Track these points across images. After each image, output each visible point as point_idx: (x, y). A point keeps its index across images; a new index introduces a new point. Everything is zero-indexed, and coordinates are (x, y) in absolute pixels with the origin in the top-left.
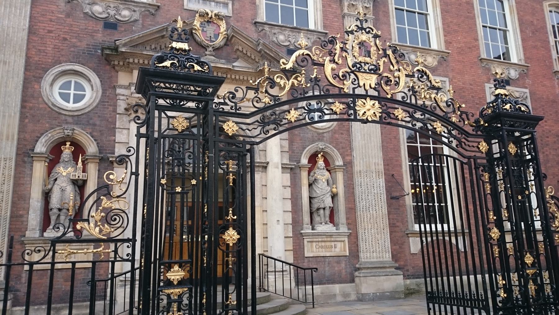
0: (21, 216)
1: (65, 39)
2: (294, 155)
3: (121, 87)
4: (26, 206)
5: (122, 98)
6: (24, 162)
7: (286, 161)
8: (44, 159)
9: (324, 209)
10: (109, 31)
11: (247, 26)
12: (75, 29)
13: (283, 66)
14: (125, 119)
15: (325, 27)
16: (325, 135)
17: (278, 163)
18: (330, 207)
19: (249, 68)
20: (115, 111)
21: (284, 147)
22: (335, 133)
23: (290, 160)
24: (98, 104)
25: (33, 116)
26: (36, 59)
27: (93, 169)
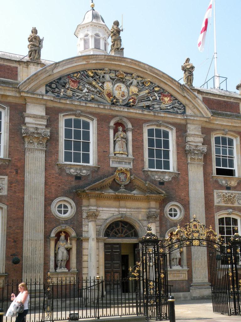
1: (59, 186)
3: (84, 206)
5: (85, 211)
10: (77, 181)
11: (140, 172)
14: (86, 220)
15: (178, 170)
19: (141, 194)
20: (82, 217)
24: (75, 214)
25: (49, 221)
26: (48, 196)
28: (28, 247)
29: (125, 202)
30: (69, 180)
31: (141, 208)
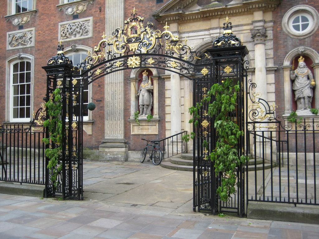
0: (128, 109)
2: (278, 59)
4: (129, 104)
6: (127, 83)
7: (271, 65)
8: (134, 81)
9: (304, 98)
10: (159, 4)
12: (143, 9)
13: (95, 50)
16: (307, 39)
17: (261, 68)
18: (309, 97)
21: (270, 55)
22: (316, 37)
23: (275, 63)
27: (156, 82)
28: (109, 91)
29: (218, 20)
30: (150, 5)
31: (242, 25)
